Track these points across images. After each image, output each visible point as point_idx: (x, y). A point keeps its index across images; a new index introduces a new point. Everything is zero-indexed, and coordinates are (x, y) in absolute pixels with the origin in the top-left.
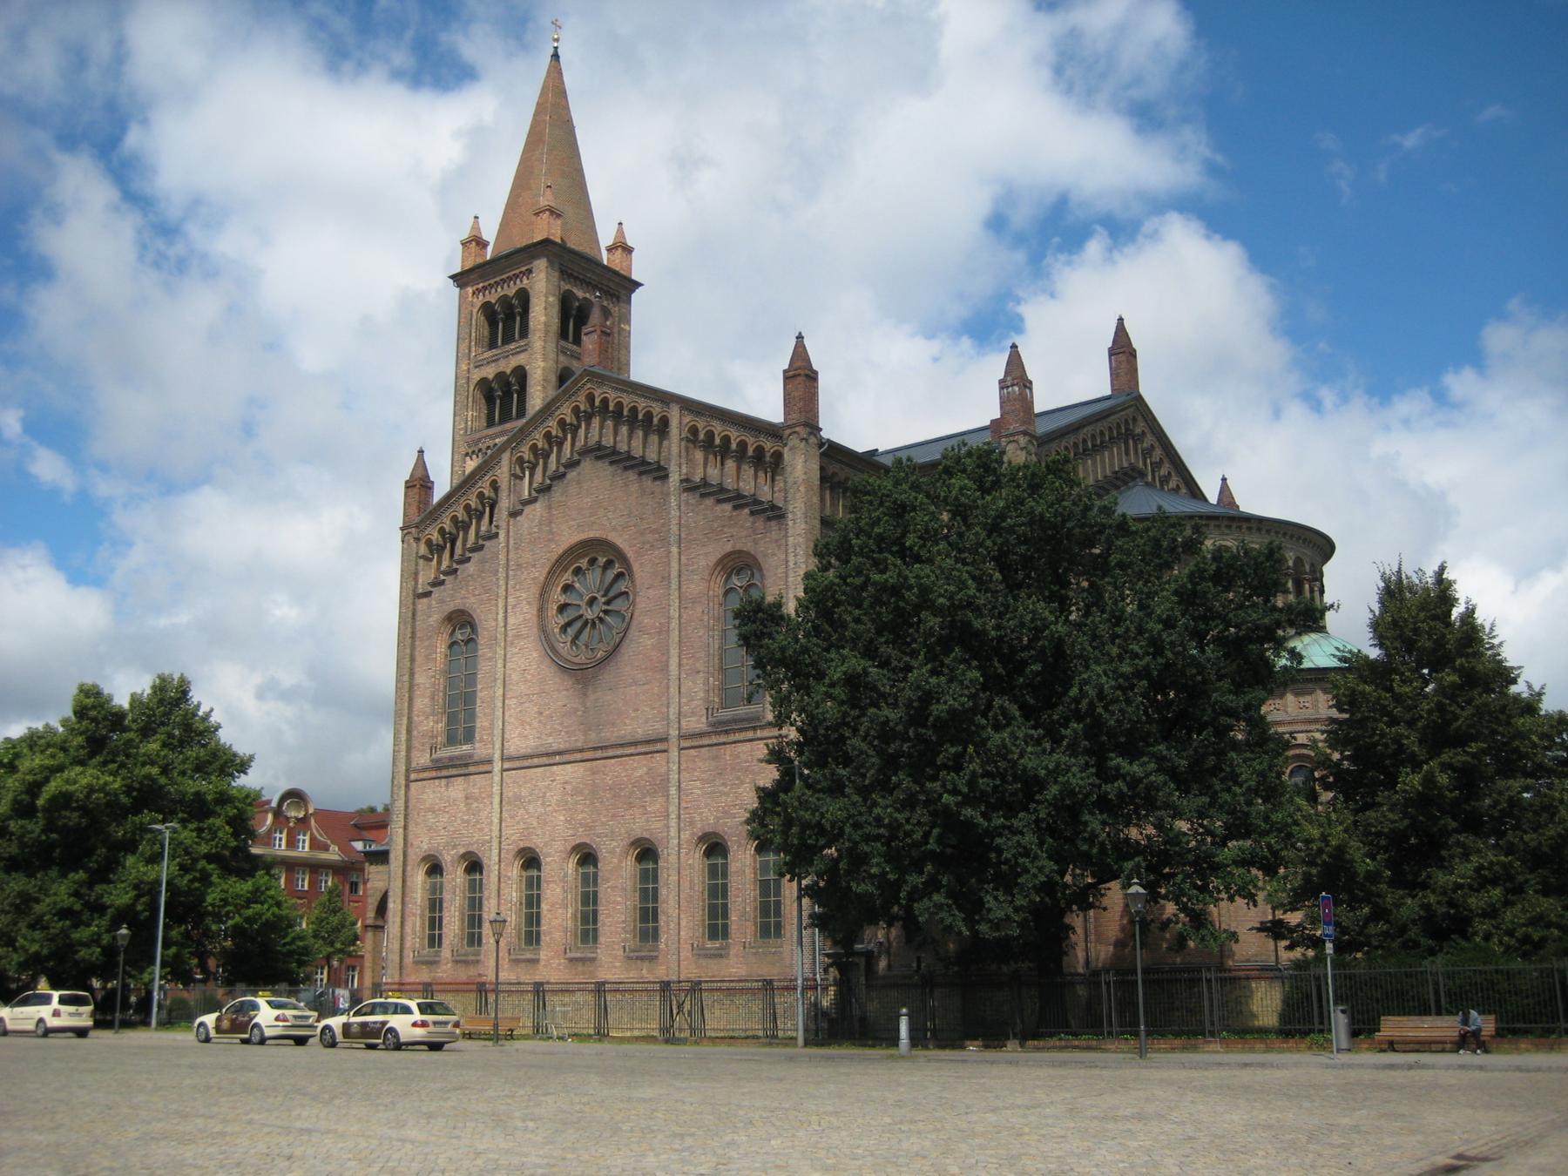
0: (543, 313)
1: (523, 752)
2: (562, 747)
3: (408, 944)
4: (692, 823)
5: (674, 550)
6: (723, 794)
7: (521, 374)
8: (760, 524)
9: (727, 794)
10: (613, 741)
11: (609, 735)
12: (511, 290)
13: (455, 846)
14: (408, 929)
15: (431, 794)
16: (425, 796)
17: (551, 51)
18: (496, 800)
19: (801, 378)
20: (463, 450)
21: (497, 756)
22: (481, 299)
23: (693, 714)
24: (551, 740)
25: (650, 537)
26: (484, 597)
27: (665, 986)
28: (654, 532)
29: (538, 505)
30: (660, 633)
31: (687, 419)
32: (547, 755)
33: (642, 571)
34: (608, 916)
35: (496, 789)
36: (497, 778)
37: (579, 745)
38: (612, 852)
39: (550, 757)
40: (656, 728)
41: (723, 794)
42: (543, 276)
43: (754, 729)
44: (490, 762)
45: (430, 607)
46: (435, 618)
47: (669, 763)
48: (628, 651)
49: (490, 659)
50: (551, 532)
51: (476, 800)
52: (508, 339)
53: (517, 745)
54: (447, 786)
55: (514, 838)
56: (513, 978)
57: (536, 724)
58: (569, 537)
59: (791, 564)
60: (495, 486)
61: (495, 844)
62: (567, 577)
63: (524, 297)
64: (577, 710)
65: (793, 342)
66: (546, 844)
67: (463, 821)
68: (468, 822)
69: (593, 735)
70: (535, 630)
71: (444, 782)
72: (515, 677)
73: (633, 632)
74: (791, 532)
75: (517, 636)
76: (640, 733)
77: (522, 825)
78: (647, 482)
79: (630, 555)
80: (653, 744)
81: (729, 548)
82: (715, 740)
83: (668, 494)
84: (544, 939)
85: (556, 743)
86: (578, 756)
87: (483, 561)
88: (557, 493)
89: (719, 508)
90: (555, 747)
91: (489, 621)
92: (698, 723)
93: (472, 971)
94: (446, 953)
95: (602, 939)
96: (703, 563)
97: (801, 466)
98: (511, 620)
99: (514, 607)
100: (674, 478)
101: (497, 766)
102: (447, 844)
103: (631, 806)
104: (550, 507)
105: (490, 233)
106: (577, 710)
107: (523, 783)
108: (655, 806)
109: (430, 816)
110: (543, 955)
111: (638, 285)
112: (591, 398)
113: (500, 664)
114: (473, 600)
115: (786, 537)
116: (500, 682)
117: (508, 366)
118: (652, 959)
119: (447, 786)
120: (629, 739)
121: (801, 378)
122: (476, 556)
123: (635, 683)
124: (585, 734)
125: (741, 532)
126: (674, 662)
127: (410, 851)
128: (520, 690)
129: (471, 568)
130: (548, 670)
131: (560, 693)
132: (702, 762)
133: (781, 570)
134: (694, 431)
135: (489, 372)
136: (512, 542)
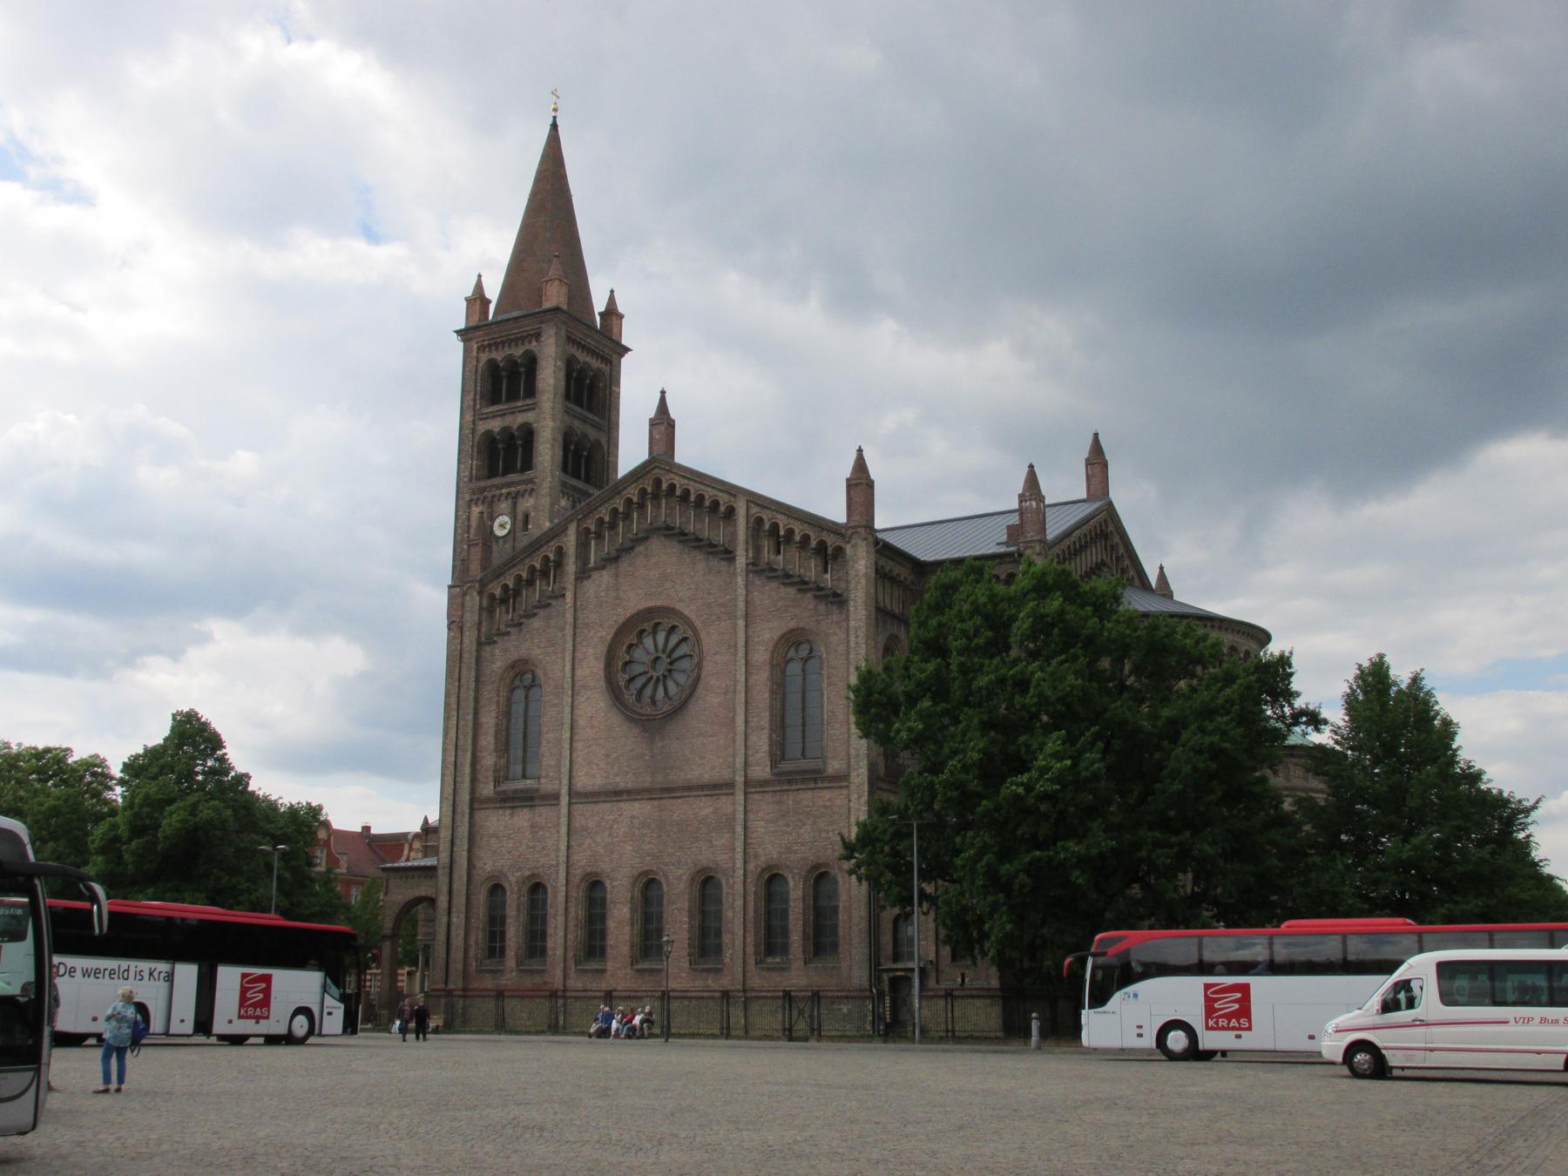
0: (549, 377)
1: (590, 788)
2: (630, 785)
3: (472, 953)
4: (756, 856)
5: (741, 623)
7: (528, 433)
8: (822, 607)
11: (678, 778)
12: (518, 352)
13: (520, 869)
14: (472, 941)
15: (494, 821)
17: (550, 121)
18: (564, 830)
19: (860, 485)
20: (467, 497)
21: (564, 790)
23: (758, 764)
26: (551, 649)
27: (788, 996)
28: (722, 605)
30: (726, 693)
31: (754, 510)
33: (711, 639)
35: (564, 820)
36: (564, 811)
37: (647, 785)
38: (679, 878)
39: (616, 795)
40: (726, 774)
42: (552, 341)
44: (556, 797)
47: (735, 804)
48: (694, 708)
49: (556, 705)
50: (617, 598)
52: (513, 396)
53: (583, 782)
54: (512, 816)
56: (579, 985)
57: (603, 765)
58: (635, 601)
59: (852, 644)
60: (560, 551)
61: (562, 868)
63: (532, 362)
65: (854, 455)
67: (528, 847)
69: (659, 778)
70: (603, 683)
71: (508, 812)
73: (700, 691)
74: (852, 617)
75: (585, 687)
78: (715, 563)
79: (698, 624)
80: (720, 788)
81: (792, 625)
83: (735, 574)
84: (610, 952)
85: (623, 782)
88: (624, 565)
89: (783, 590)
90: (622, 786)
91: (554, 669)
93: (538, 979)
94: (510, 962)
96: (767, 635)
97: (861, 562)
98: (579, 672)
100: (741, 560)
101: (564, 800)
104: (617, 576)
105: (493, 291)
107: (587, 815)
108: (721, 840)
109: (493, 841)
110: (610, 966)
111: (627, 350)
112: (658, 482)
113: (568, 710)
115: (847, 619)
116: (567, 727)
118: (718, 971)
119: (512, 816)
121: (860, 485)
122: (541, 612)
125: (803, 613)
127: (474, 872)
128: (585, 734)
129: (536, 623)
130: (615, 718)
131: (627, 739)
132: (765, 806)
133: (842, 648)
134: (760, 521)
135: (495, 425)
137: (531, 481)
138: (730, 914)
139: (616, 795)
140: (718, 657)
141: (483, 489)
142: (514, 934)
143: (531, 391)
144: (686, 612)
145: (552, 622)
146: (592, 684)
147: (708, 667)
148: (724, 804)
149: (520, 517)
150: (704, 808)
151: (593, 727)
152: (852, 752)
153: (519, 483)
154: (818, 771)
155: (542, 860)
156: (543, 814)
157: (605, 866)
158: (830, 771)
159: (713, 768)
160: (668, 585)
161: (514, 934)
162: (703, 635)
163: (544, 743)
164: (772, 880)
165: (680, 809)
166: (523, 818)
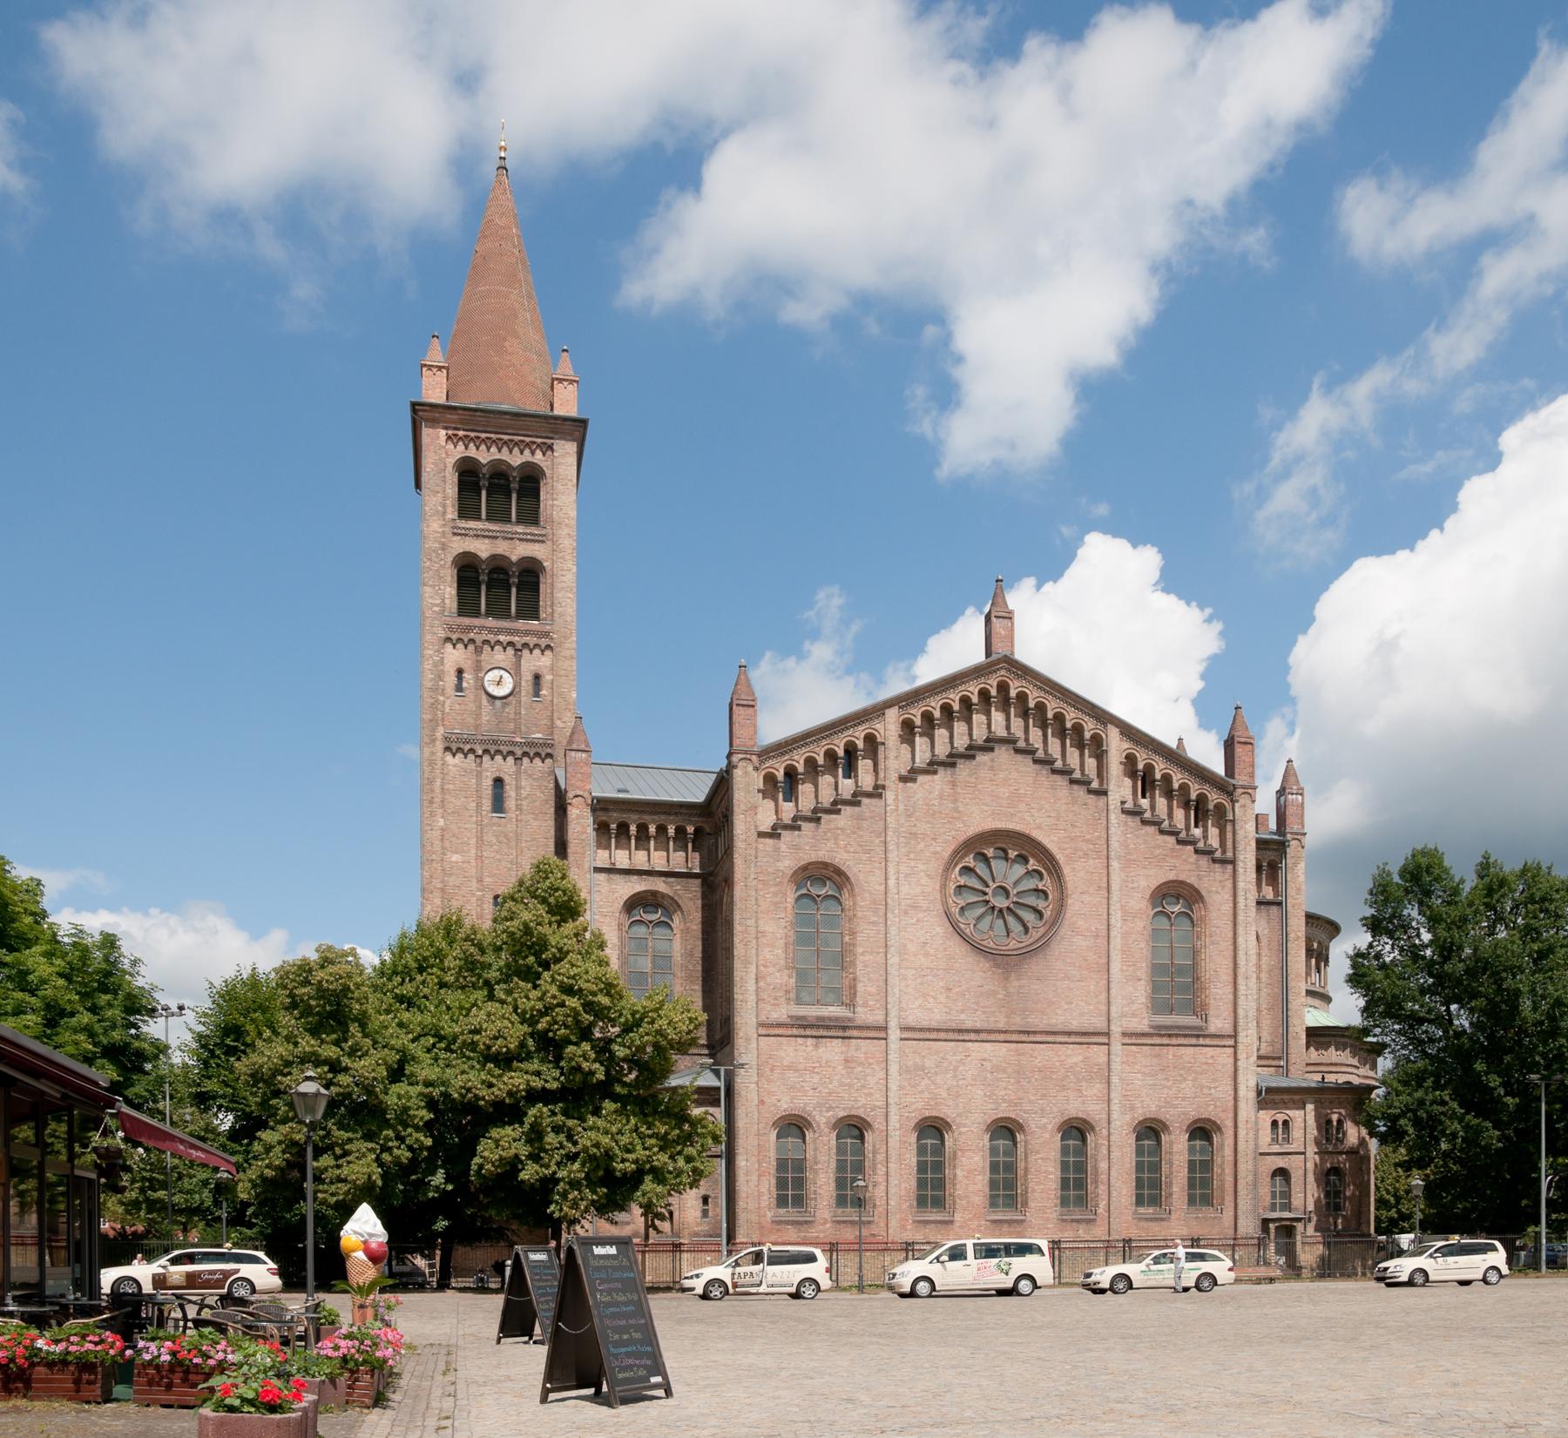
1: (925, 1024)
2: (978, 1025)
4: (1132, 1108)
6: (1164, 1087)
9: (1169, 1088)
10: (1041, 1027)
11: (1037, 1021)
12: (516, 459)
13: (830, 1109)
16: (783, 1054)
22: (459, 451)
23: (1134, 1015)
24: (963, 1017)
25: (1085, 846)
28: (1087, 841)
29: (936, 777)
31: (1126, 745)
32: (960, 1031)
33: (1074, 874)
34: (1038, 1183)
38: (1044, 1127)
39: (960, 1033)
40: (1099, 1023)
41: (1164, 1087)
43: (1198, 1036)
45: (777, 850)
46: (788, 864)
48: (1057, 949)
50: (956, 810)
51: (861, 1064)
53: (916, 1016)
54: (816, 1046)
55: (920, 1107)
57: (942, 998)
62: (970, 861)
64: (995, 993)
66: (959, 1115)
68: (850, 1085)
69: (1018, 1020)
72: (912, 948)
73: (1064, 930)
76: (1075, 1025)
77: (926, 1095)
79: (1060, 857)
80: (1085, 1036)
81: (1172, 876)
82: (1158, 1041)
86: (1002, 1037)
87: (860, 818)
89: (1161, 838)
90: (969, 1025)
92: (1143, 1026)
95: (1032, 1204)
96: (1143, 883)
98: (905, 889)
99: (908, 875)
101: (894, 1034)
102: (819, 1105)
103: (1064, 1088)
104: (954, 784)
106: (995, 993)
109: (790, 1074)
110: (957, 1217)
114: (845, 856)
117: (517, 551)
119: (816, 1046)
120: (1060, 1028)
122: (847, 811)
123: (1067, 977)
124: (1008, 1017)
126: (1116, 967)
130: (957, 948)
131: (974, 973)
132: (1144, 1057)
135: (483, 549)
136: (902, 807)
137: (546, 635)
138: (1103, 1165)
139: (960, 1033)
140: (1086, 898)
141: (470, 629)
142: (822, 1183)
143: (531, 515)
144: (1046, 842)
145: (865, 824)
146: (924, 905)
147: (1074, 905)
148: (1098, 1054)
149: (527, 677)
150: (1074, 1055)
151: (927, 954)
152: (1241, 1012)
153: (527, 633)
154: (1201, 1028)
155: (863, 1101)
156: (862, 1049)
157: (947, 1111)
158: (1212, 1029)
159: (1082, 1015)
160: (1022, 807)
161: (822, 1183)
162: (1066, 870)
163: (860, 966)
164: (1150, 1131)
165: (1042, 1055)
166: (832, 1050)
